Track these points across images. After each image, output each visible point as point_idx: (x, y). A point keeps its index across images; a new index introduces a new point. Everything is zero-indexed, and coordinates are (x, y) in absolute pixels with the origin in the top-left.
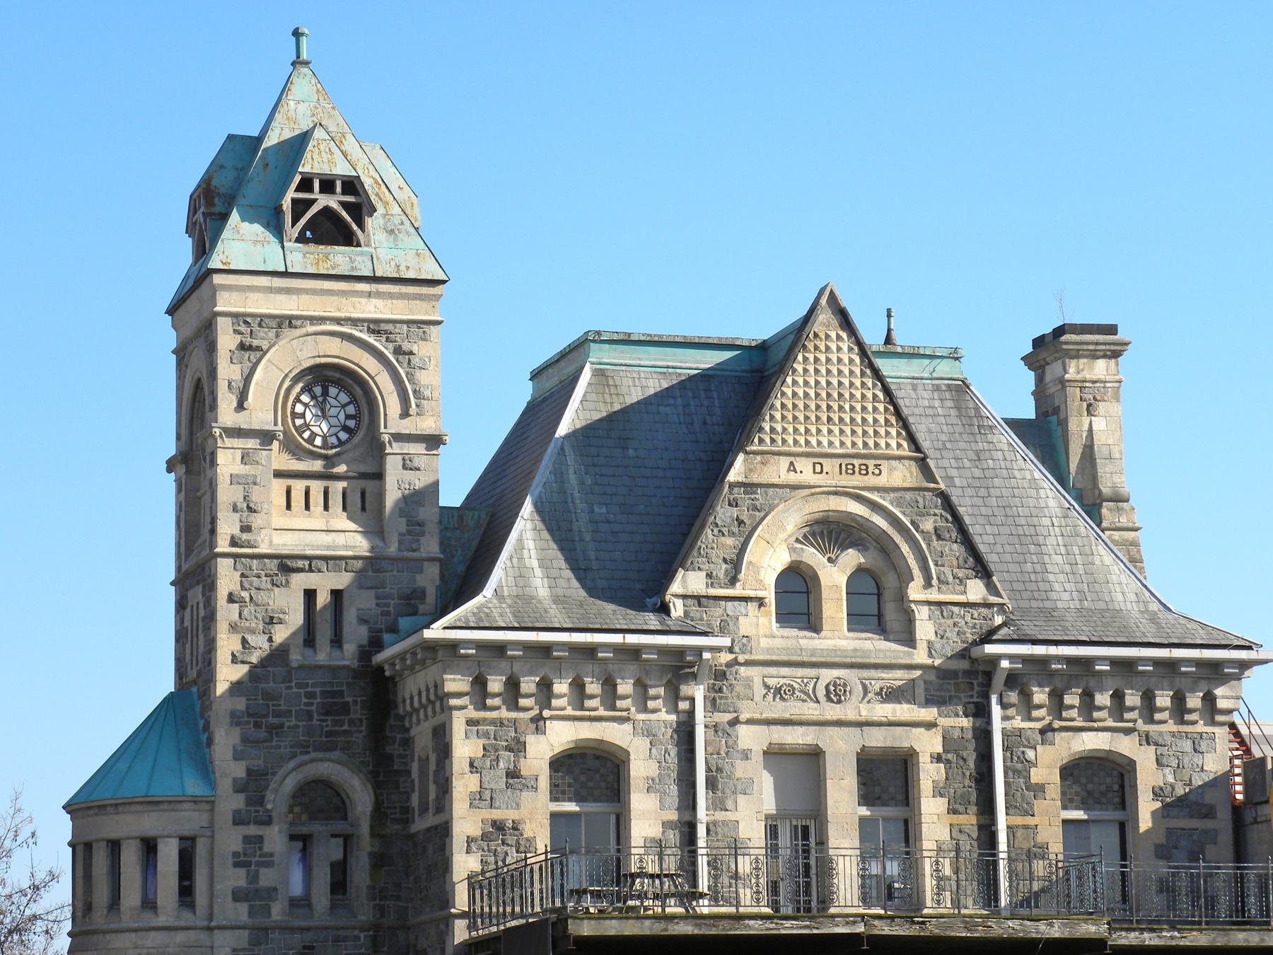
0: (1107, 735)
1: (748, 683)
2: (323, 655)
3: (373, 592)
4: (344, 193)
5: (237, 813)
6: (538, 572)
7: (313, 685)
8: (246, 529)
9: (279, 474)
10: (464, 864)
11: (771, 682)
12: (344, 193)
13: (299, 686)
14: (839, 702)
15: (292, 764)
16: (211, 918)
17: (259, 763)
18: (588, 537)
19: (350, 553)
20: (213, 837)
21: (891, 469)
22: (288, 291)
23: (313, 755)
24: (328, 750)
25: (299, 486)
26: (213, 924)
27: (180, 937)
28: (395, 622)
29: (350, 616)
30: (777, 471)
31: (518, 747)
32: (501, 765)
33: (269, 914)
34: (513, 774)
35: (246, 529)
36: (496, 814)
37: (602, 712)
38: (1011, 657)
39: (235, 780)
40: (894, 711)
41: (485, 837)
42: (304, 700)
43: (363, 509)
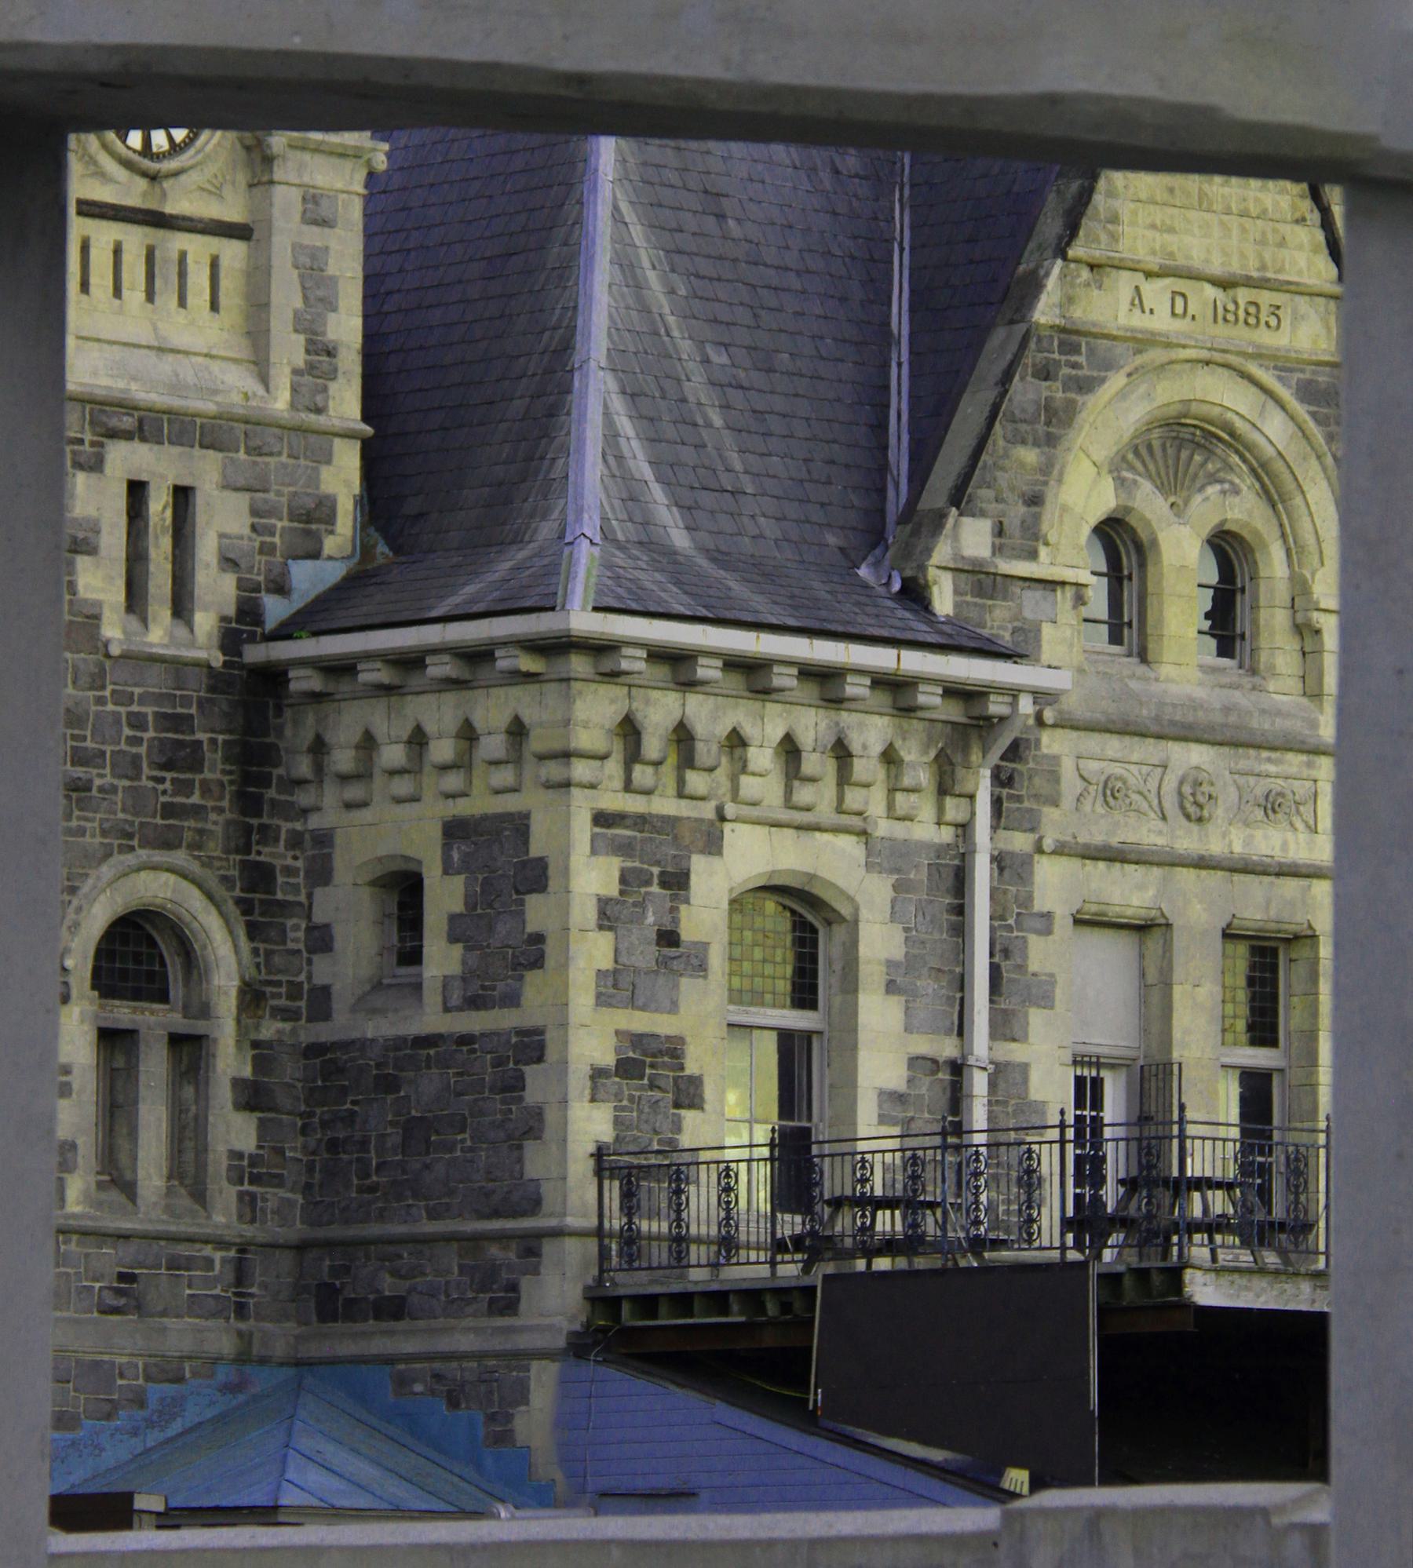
2: (159, 634)
3: (247, 496)
6: (657, 492)
7: (142, 700)
10: (590, 1124)
11: (1092, 767)
14: (1200, 820)
15: (106, 871)
18: (717, 421)
21: (1297, 318)
23: (143, 854)
24: (168, 845)
28: (285, 573)
29: (206, 550)
30: (1109, 307)
31: (677, 882)
32: (650, 919)
34: (668, 938)
36: (640, 1022)
37: (825, 811)
40: (1285, 846)
41: (626, 1068)
42: (127, 732)
43: (214, 306)
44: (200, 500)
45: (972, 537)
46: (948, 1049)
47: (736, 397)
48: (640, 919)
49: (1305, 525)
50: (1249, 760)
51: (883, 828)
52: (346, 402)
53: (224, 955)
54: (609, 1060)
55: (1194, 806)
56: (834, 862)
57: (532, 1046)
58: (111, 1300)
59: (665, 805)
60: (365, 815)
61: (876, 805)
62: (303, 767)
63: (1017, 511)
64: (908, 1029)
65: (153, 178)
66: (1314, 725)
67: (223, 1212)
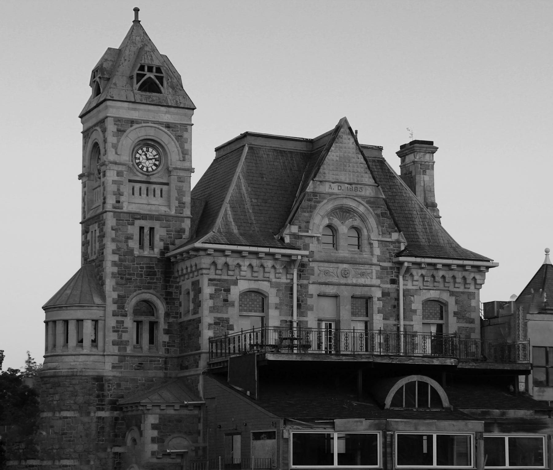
0: (439, 292)
1: (313, 269)
2: (146, 252)
4: (157, 72)
5: (114, 311)
6: (233, 223)
7: (143, 264)
8: (118, 202)
9: (130, 181)
10: (207, 334)
12: (157, 72)
13: (137, 264)
15: (135, 294)
16: (104, 351)
17: (122, 293)
18: (251, 211)
19: (157, 213)
20: (105, 320)
22: (135, 109)
23: (143, 291)
25: (137, 186)
26: (105, 353)
27: (92, 358)
28: (174, 241)
29: (157, 238)
30: (325, 188)
31: (228, 291)
33: (126, 350)
34: (226, 300)
35: (118, 202)
36: (219, 315)
37: (261, 277)
38: (408, 262)
39: (113, 299)
41: (216, 323)
42: (140, 270)
43: (161, 196)
44: (155, 229)
45: (294, 229)
46: (289, 319)
47: (256, 207)
48: (219, 297)
49: (369, 225)
50: (357, 266)
51: (274, 280)
52: (187, 212)
53: (161, 308)
54: (212, 322)
55: (345, 275)
56: (264, 286)
57: (199, 321)
58: (136, 367)
59: (226, 277)
60: (184, 282)
61: (272, 276)
62: (176, 275)
63: (303, 225)
64: (280, 315)
65: (148, 175)
66: (372, 260)
67: (162, 352)
